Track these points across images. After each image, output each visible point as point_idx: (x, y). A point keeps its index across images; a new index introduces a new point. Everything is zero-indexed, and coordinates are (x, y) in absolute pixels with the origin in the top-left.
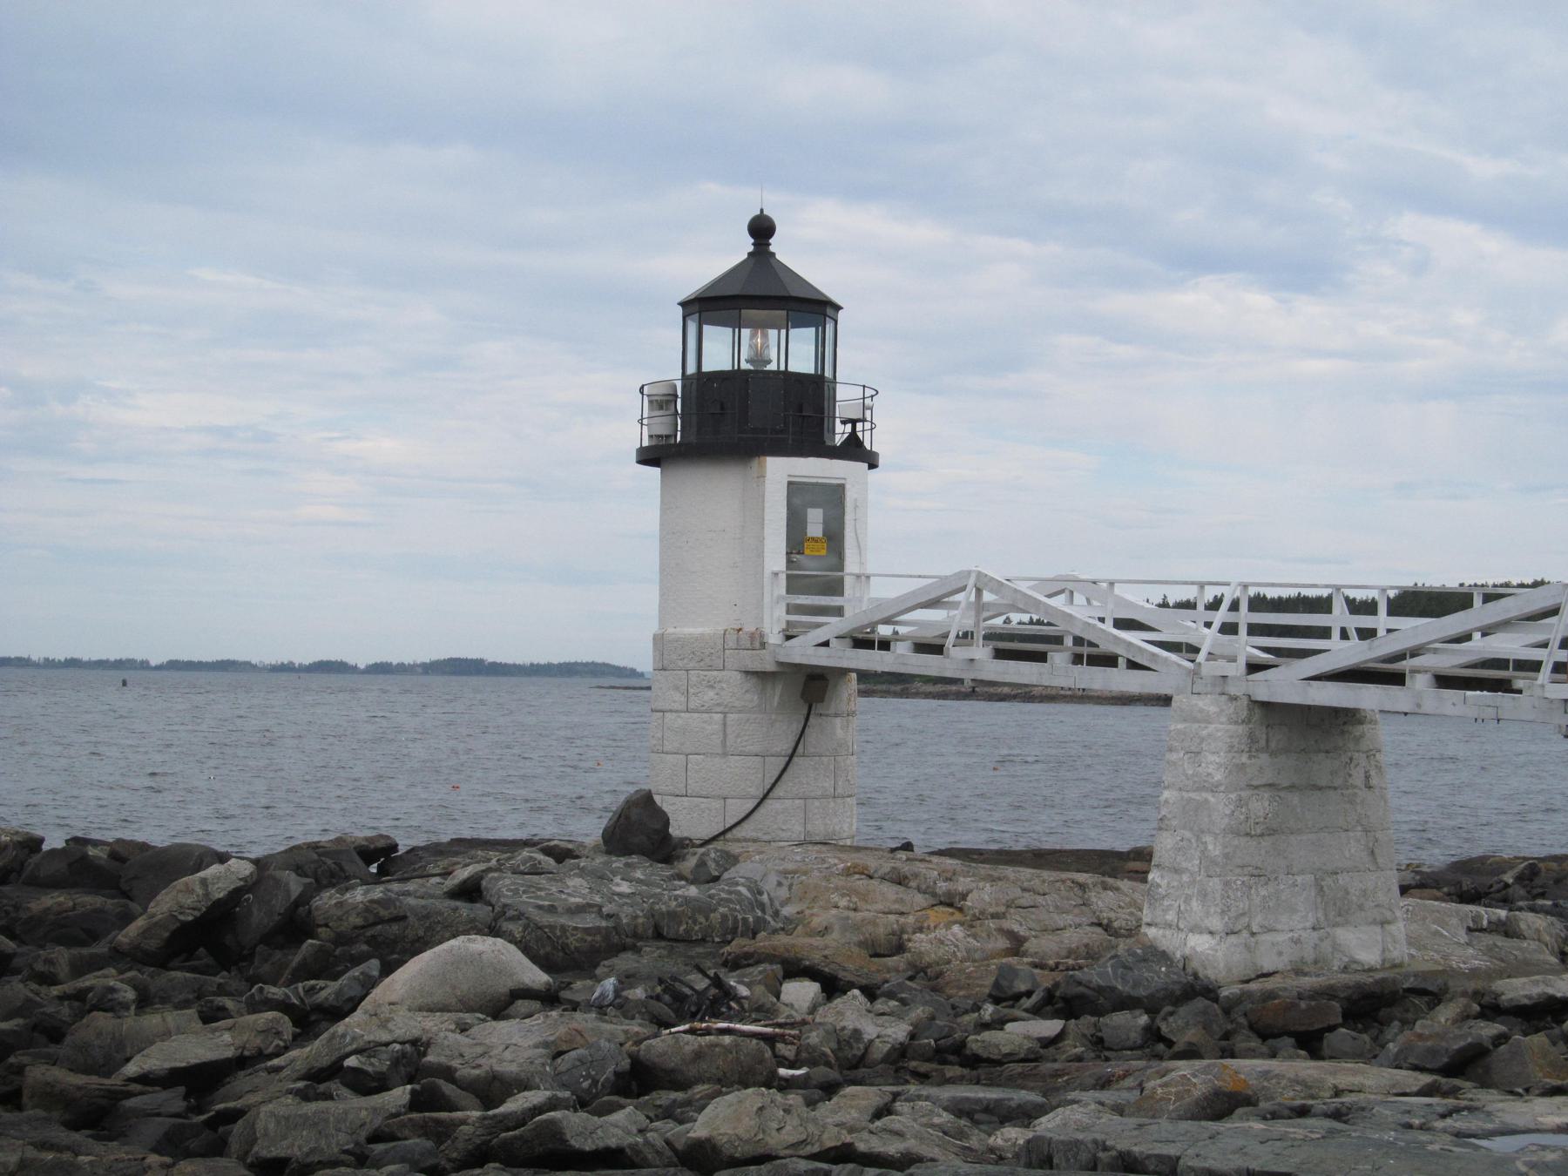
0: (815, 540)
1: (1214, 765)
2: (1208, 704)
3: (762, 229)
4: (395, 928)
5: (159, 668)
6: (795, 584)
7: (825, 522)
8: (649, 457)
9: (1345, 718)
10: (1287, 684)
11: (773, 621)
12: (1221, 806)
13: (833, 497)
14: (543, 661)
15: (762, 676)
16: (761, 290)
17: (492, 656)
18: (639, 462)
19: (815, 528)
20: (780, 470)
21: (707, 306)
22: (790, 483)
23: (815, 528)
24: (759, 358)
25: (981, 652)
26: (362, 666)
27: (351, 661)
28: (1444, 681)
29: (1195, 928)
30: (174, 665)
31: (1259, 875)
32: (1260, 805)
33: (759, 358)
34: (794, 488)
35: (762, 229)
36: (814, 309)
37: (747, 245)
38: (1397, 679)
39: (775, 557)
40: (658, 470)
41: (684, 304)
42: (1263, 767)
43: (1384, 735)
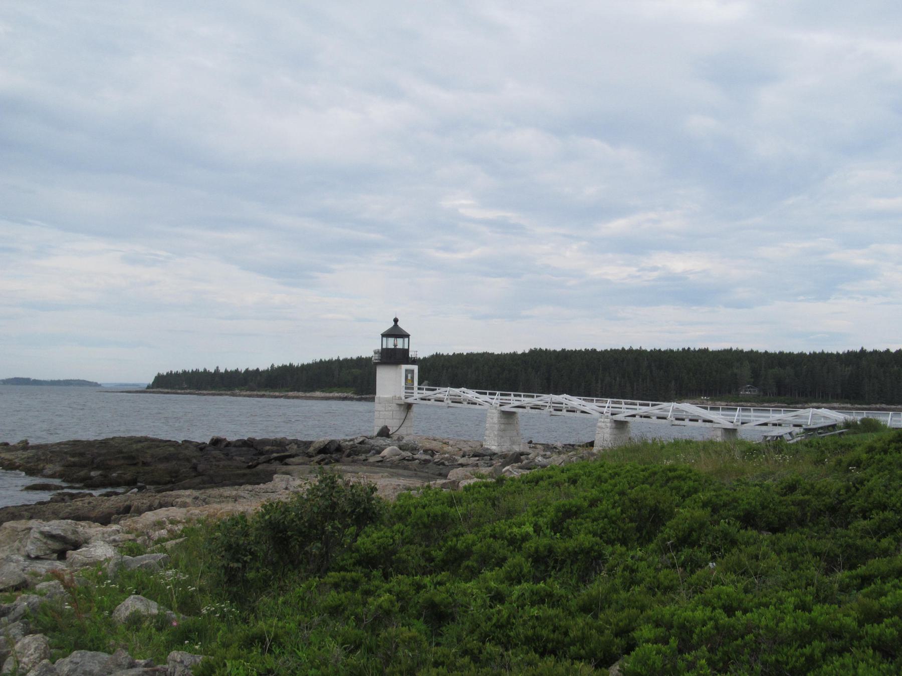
1: (496, 420)
2: (494, 411)
3: (396, 321)
6: (406, 388)
9: (514, 413)
10: (506, 408)
11: (403, 395)
12: (497, 426)
13: (412, 371)
14: (56, 379)
15: (400, 405)
16: (396, 332)
17: (33, 377)
19: (409, 378)
20: (404, 367)
21: (386, 335)
23: (409, 378)
24: (395, 346)
25: (450, 402)
28: (532, 408)
29: (492, 445)
31: (502, 437)
32: (502, 426)
34: (406, 370)
35: (396, 321)
36: (405, 336)
37: (393, 323)
38: (524, 407)
39: (403, 384)
42: (503, 421)
43: (519, 416)
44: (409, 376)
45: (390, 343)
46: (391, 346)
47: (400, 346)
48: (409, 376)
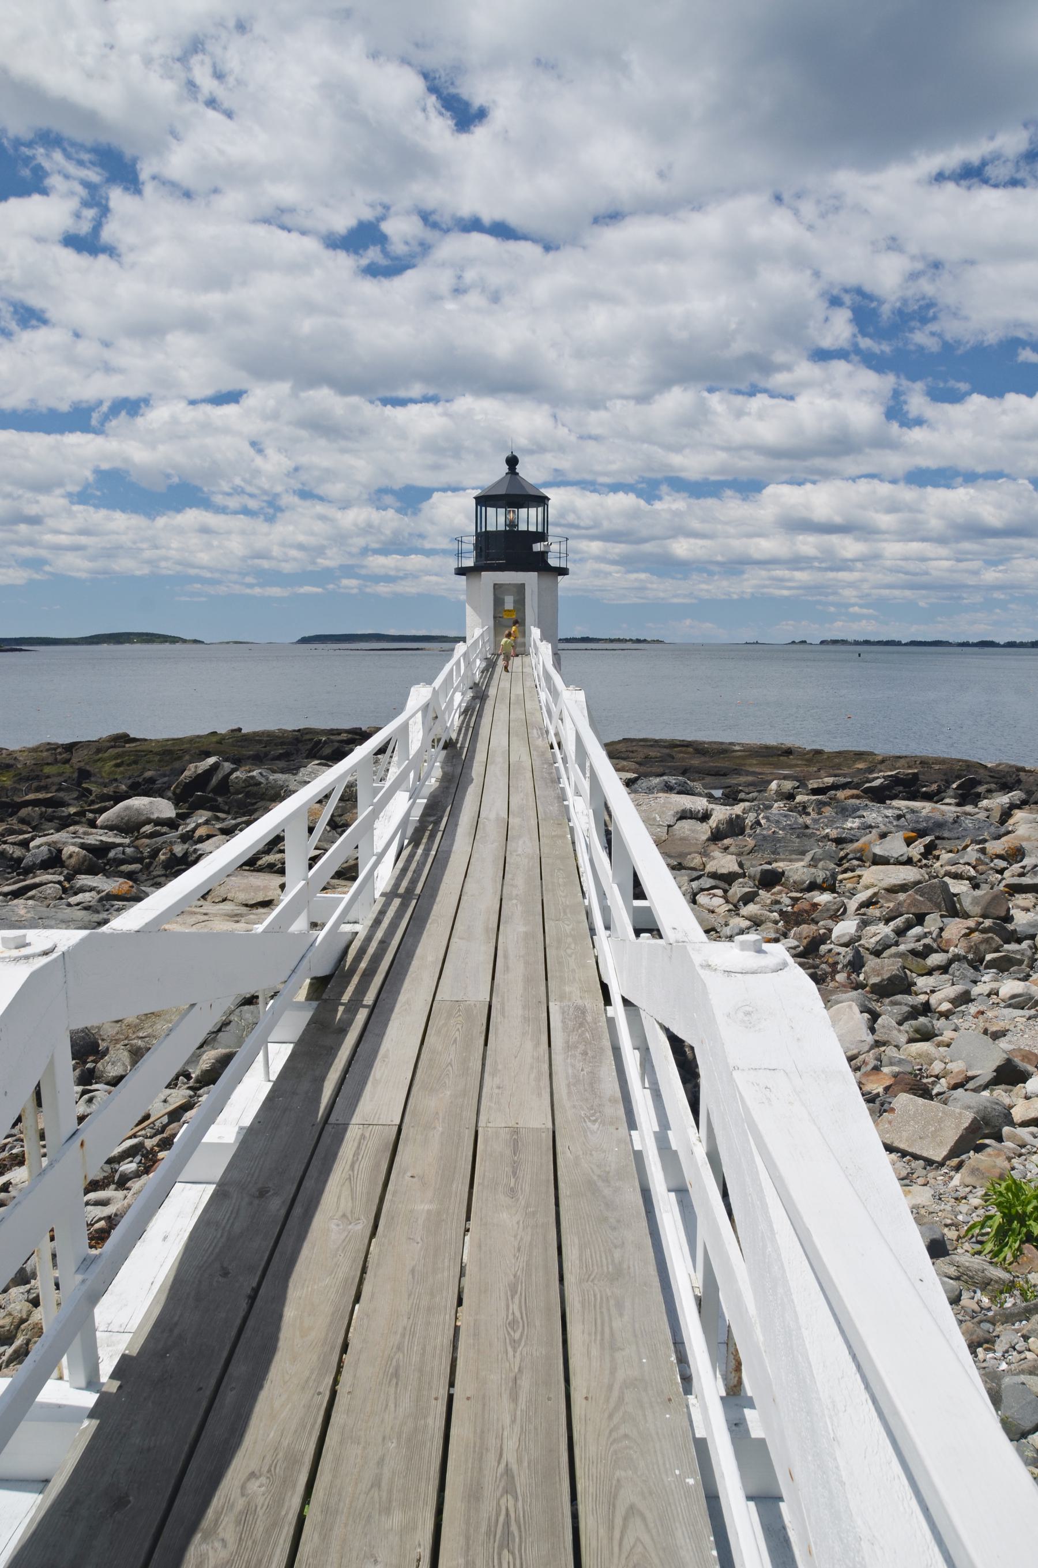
0: (509, 611)
3: (512, 462)
4: (255, 788)
5: (906, 644)
7: (515, 602)
8: (461, 571)
18: (457, 574)
20: (490, 578)
22: (495, 585)
24: (512, 524)
26: (1002, 643)
27: (997, 640)
30: (913, 643)
33: (512, 524)
34: (496, 587)
35: (512, 462)
37: (505, 468)
40: (464, 577)
41: (476, 498)
44: (509, 603)
45: (496, 519)
46: (501, 527)
47: (522, 527)
48: (509, 603)
